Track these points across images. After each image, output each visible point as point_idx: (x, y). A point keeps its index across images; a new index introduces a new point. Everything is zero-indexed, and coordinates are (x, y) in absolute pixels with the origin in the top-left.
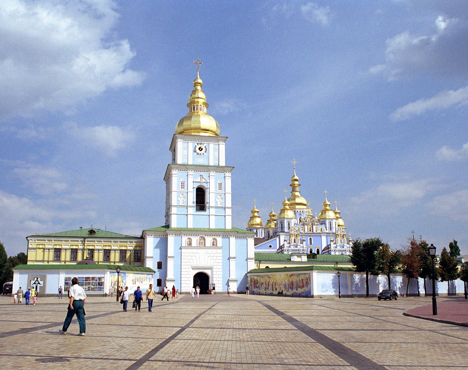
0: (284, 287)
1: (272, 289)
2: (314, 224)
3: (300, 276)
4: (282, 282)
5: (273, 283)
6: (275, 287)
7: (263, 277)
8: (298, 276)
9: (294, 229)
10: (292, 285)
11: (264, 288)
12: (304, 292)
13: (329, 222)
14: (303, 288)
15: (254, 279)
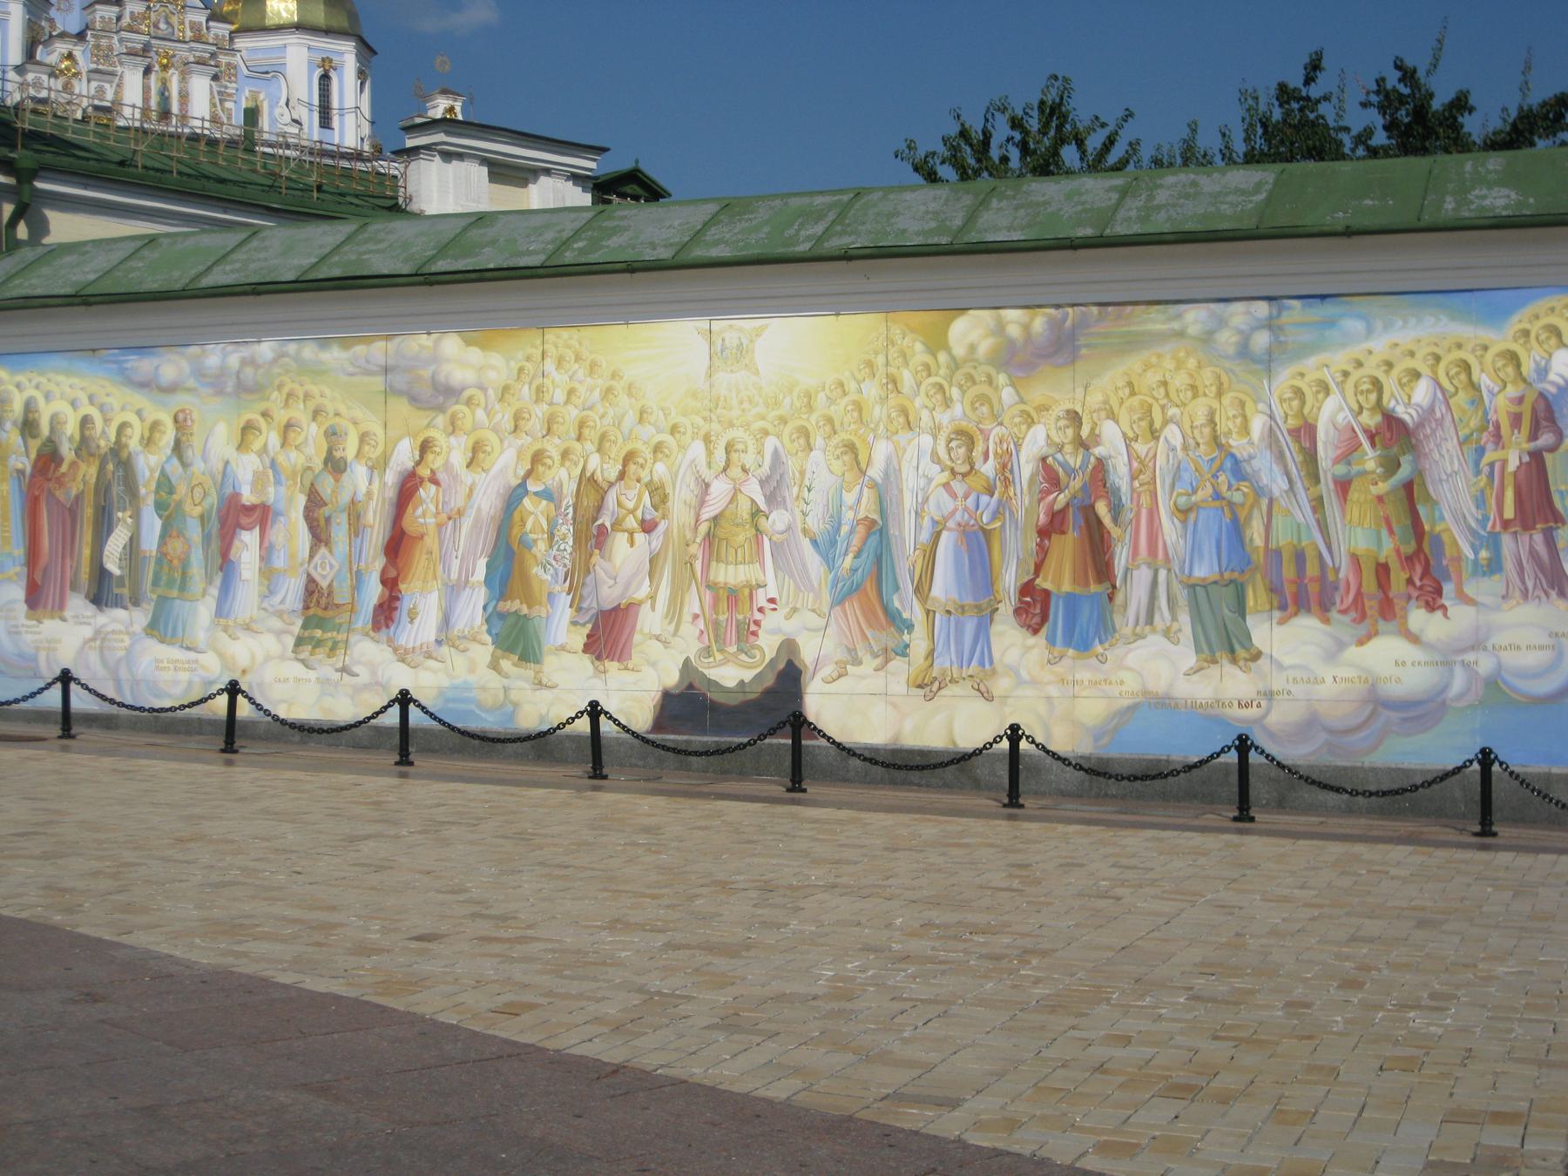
0: (844, 594)
1: (493, 617)
2: (200, 62)
3: (1340, 359)
4: (773, 498)
5: (513, 499)
6: (578, 577)
7: (245, 389)
8: (1244, 351)
9: (70, 56)
10: (1066, 547)
11: (291, 591)
12: (1458, 683)
13: (318, 58)
14: (1418, 617)
15: (28, 426)
